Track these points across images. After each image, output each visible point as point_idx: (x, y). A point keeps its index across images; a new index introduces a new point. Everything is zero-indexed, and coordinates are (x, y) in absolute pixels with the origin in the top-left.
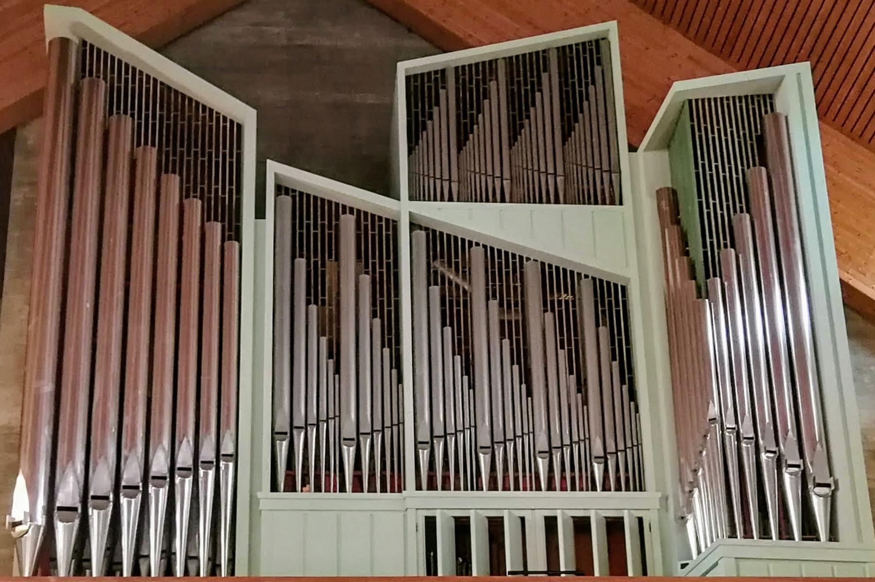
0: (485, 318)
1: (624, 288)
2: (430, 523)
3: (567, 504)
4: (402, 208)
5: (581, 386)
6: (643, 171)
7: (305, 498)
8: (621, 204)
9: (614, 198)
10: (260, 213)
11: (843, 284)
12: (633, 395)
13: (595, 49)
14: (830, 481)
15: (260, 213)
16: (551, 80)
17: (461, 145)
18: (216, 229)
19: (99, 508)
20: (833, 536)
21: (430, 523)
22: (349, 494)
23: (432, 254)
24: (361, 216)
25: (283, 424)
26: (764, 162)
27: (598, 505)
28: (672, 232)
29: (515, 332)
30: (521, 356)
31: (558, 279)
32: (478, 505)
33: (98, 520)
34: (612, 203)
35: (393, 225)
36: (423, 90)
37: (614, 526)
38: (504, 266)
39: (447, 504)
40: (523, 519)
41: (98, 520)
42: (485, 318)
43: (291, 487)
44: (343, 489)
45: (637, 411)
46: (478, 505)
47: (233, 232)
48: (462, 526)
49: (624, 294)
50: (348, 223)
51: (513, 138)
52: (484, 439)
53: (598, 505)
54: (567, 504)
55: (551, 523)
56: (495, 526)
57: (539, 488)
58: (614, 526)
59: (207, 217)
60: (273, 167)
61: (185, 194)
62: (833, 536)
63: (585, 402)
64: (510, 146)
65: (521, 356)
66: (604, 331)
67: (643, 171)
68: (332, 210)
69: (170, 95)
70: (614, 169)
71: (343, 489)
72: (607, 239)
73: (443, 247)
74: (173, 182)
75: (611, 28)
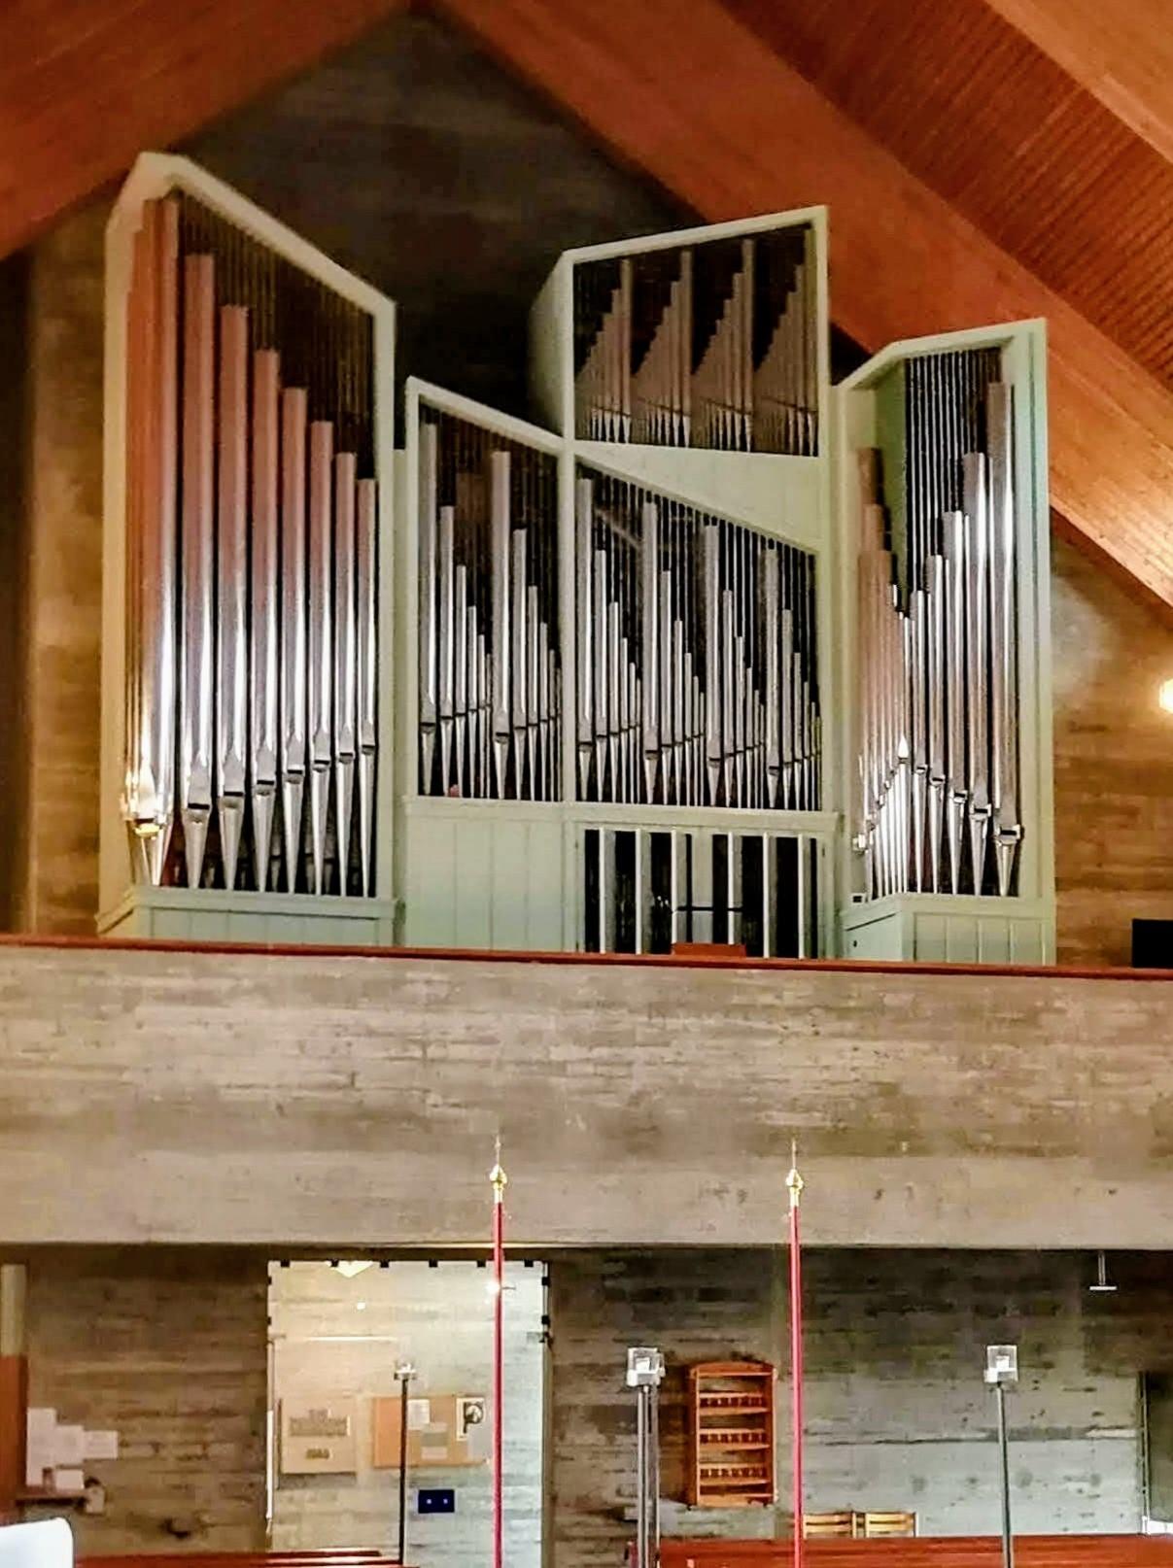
0: (656, 588)
1: (812, 558)
2: (592, 837)
3: (739, 822)
4: (566, 448)
5: (760, 682)
6: (843, 410)
7: (452, 805)
8: (816, 454)
9: (809, 449)
10: (400, 442)
11: (1052, 509)
12: (814, 695)
14: (1017, 828)
15: (400, 442)
17: (635, 368)
18: (349, 461)
19: (232, 806)
20: (1013, 891)
21: (592, 837)
22: (501, 801)
23: (597, 501)
25: (429, 716)
26: (983, 447)
27: (769, 824)
28: (872, 512)
29: (690, 607)
32: (642, 819)
34: (806, 453)
35: (552, 461)
36: (594, 285)
37: (786, 848)
38: (682, 525)
39: (611, 817)
40: (689, 837)
42: (656, 588)
43: (437, 790)
44: (494, 795)
45: (818, 714)
46: (642, 819)
47: (366, 469)
49: (812, 568)
50: (502, 461)
52: (651, 743)
54: (739, 822)
55: (719, 842)
57: (707, 803)
59: (339, 447)
60: (417, 388)
61: (312, 416)
62: (1013, 891)
63: (763, 700)
64: (693, 372)
66: (787, 615)
67: (843, 410)
68: (482, 440)
69: (289, 275)
70: (810, 411)
71: (494, 795)
72: (799, 498)
73: (609, 492)
74: (299, 397)
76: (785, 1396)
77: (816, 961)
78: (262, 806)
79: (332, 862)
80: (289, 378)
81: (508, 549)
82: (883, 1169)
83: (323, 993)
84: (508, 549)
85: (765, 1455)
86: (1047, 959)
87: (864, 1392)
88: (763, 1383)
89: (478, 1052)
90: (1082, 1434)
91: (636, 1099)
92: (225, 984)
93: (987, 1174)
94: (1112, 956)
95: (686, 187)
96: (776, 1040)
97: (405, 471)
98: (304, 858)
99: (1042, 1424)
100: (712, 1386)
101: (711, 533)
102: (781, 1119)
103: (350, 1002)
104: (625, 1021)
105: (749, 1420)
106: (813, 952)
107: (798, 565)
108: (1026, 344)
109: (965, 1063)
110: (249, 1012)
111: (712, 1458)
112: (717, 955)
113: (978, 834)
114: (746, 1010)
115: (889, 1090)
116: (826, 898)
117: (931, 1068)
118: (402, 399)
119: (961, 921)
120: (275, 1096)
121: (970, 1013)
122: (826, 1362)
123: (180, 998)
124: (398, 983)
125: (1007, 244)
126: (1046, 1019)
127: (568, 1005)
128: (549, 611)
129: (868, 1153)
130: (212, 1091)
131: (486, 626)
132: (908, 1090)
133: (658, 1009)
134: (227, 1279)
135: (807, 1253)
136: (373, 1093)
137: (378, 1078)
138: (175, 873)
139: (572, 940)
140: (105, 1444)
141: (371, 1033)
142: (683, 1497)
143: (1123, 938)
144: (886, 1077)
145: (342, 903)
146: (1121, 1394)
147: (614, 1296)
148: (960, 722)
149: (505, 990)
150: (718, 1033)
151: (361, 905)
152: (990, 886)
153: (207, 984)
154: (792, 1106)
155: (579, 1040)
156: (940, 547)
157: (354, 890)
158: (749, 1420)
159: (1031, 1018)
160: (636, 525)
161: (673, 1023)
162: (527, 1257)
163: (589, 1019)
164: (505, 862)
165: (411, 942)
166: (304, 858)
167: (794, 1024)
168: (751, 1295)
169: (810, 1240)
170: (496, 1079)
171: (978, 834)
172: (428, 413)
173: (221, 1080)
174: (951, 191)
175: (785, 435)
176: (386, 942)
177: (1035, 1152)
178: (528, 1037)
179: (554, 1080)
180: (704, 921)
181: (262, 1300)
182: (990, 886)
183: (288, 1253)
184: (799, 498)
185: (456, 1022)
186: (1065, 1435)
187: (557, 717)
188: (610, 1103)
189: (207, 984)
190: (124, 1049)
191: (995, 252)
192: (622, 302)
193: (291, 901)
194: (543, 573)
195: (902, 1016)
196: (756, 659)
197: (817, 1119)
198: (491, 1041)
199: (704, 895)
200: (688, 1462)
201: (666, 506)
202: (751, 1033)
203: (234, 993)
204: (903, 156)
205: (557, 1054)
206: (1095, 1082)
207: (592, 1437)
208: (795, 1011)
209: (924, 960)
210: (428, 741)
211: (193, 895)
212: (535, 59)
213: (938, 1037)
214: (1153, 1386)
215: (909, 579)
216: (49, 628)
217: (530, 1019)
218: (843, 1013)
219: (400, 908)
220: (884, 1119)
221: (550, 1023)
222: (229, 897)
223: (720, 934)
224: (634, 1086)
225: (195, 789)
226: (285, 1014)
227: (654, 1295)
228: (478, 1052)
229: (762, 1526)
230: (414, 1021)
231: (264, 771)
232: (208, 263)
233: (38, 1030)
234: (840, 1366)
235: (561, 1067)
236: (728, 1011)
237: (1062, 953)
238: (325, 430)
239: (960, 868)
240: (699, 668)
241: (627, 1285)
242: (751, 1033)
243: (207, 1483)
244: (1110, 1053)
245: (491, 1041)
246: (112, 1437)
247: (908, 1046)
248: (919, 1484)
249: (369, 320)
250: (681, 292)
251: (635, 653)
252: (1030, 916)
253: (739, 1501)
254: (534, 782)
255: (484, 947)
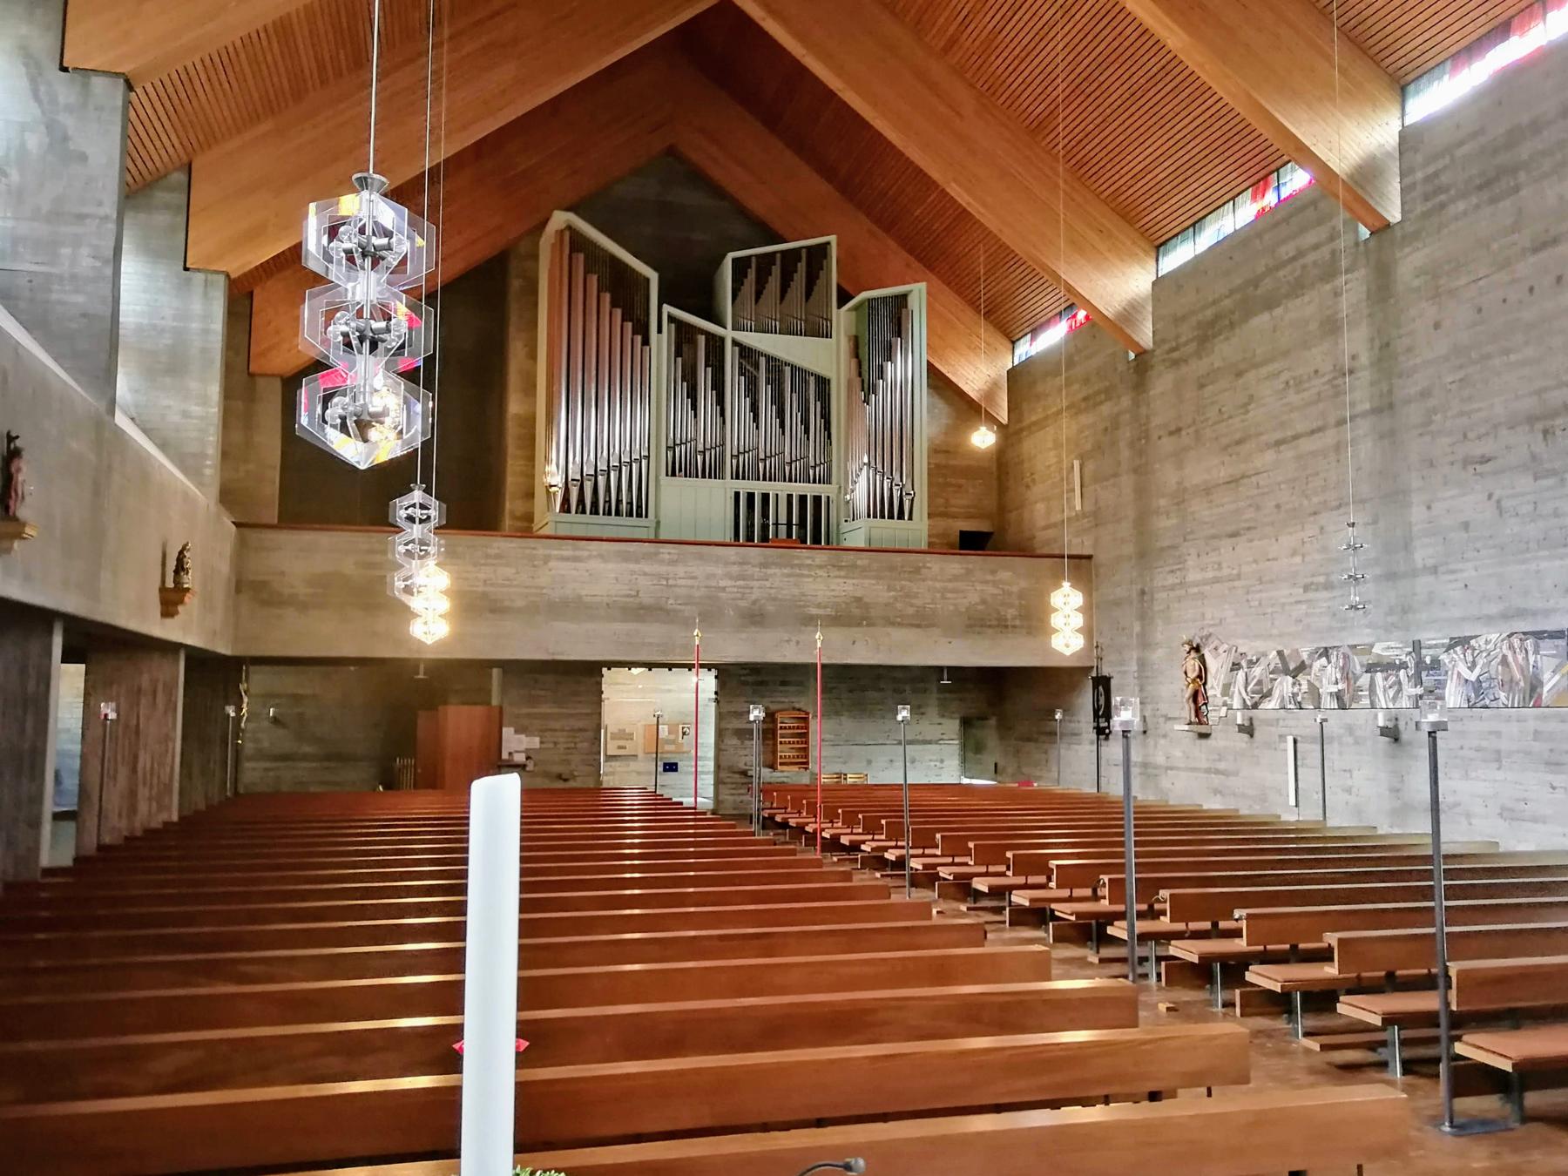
2: (737, 495)
4: (729, 334)
5: (807, 431)
6: (842, 319)
7: (679, 480)
9: (828, 335)
10: (660, 331)
12: (829, 437)
13: (823, 249)
15: (660, 331)
16: (802, 267)
18: (639, 338)
20: (910, 518)
21: (737, 495)
23: (741, 356)
24: (710, 337)
25: (671, 444)
27: (810, 490)
28: (854, 361)
30: (781, 414)
31: (800, 373)
32: (758, 487)
33: (588, 486)
35: (722, 340)
36: (740, 267)
37: (817, 499)
39: (745, 486)
41: (588, 486)
43: (674, 474)
46: (758, 487)
47: (646, 342)
48: (751, 496)
50: (702, 339)
51: (782, 298)
52: (762, 456)
53: (810, 490)
55: (790, 497)
56: (765, 497)
58: (817, 499)
59: (634, 333)
60: (667, 308)
62: (910, 518)
65: (781, 414)
67: (842, 319)
72: (822, 355)
73: (746, 353)
74: (618, 312)
75: (833, 239)
76: (814, 726)
77: (829, 546)
78: (601, 480)
79: (630, 503)
80: (614, 304)
81: (704, 376)
82: (855, 632)
83: (626, 557)
84: (704, 376)
85: (806, 750)
86: (924, 546)
87: (847, 724)
88: (806, 720)
89: (690, 582)
90: (936, 742)
91: (754, 602)
92: (586, 553)
93: (898, 634)
94: (952, 546)
95: (778, 225)
96: (813, 579)
97: (661, 343)
98: (619, 501)
99: (920, 738)
100: (785, 721)
101: (788, 369)
102: (814, 611)
103: (637, 561)
104: (750, 570)
105: (799, 735)
106: (828, 542)
107: (823, 383)
108: (918, 293)
109: (889, 590)
110: (595, 565)
111: (784, 751)
112: (788, 543)
113: (896, 495)
114: (800, 566)
115: (859, 600)
116: (833, 520)
117: (875, 591)
118: (662, 314)
119: (889, 530)
120: (606, 600)
121: (892, 568)
122: (832, 711)
123: (567, 559)
124: (657, 554)
125: (911, 252)
126: (924, 571)
127: (727, 564)
128: (720, 401)
129: (849, 625)
130: (580, 597)
131: (694, 407)
132: (866, 600)
133: (764, 565)
134: (587, 675)
135: (823, 666)
136: (646, 599)
137: (648, 590)
138: (566, 507)
139: (729, 537)
140: (535, 742)
141: (645, 574)
142: (772, 767)
143: (956, 538)
144: (858, 594)
145: (634, 520)
146: (952, 726)
147: (745, 683)
148: (890, 448)
149: (701, 557)
150: (789, 576)
151: (642, 521)
152: (901, 516)
153: (578, 553)
154: (819, 606)
155: (731, 578)
156: (882, 375)
157: (639, 515)
158: (799, 735)
159: (917, 570)
160: (757, 367)
161: (770, 571)
162: (709, 667)
163: (735, 569)
164: (703, 504)
165: (662, 537)
166: (619, 501)
167: (820, 572)
168: (800, 684)
169: (825, 661)
170: (697, 594)
171: (896, 495)
172: (671, 319)
173: (583, 593)
174: (887, 230)
175: (819, 330)
176: (652, 537)
177: (918, 626)
178: (709, 577)
179: (722, 595)
180: (783, 529)
181: (600, 684)
182: (901, 516)
183: (611, 665)
184: (822, 355)
185: (680, 570)
186: (930, 742)
187: (723, 445)
188: (743, 604)
189: (578, 553)
190: (544, 579)
191: (905, 254)
192: (752, 274)
193: (613, 519)
194: (718, 386)
195: (864, 569)
196: (805, 422)
197: (829, 611)
198: (694, 578)
199: (783, 519)
200: (774, 752)
201: (769, 358)
202: (802, 575)
203: (590, 557)
204: (868, 215)
205: (722, 584)
206: (943, 598)
207: (735, 741)
208: (820, 567)
209: (873, 547)
210: (670, 454)
211: (573, 516)
212: (716, 173)
213: (878, 578)
214: (966, 723)
215: (869, 389)
216: (514, 406)
217: (711, 569)
218: (841, 568)
219: (658, 523)
220: (856, 612)
221: (719, 571)
222: (587, 518)
223: (789, 535)
224: (754, 597)
225: (574, 473)
226: (610, 566)
227: (762, 683)
228: (690, 582)
229: (805, 779)
230: (663, 569)
231: (602, 466)
232: (581, 256)
233: (509, 572)
234: (837, 713)
235: (724, 589)
236: (792, 566)
237: (930, 544)
238: (629, 325)
239: (889, 508)
240: (782, 425)
241: (750, 679)
242: (802, 575)
243: (576, 758)
244: (950, 585)
245: (694, 578)
246: (537, 739)
247: (867, 582)
248: (869, 762)
249: (648, 280)
250: (776, 270)
251: (756, 419)
252: (917, 529)
253: (795, 768)
254: (713, 471)
255: (692, 539)
